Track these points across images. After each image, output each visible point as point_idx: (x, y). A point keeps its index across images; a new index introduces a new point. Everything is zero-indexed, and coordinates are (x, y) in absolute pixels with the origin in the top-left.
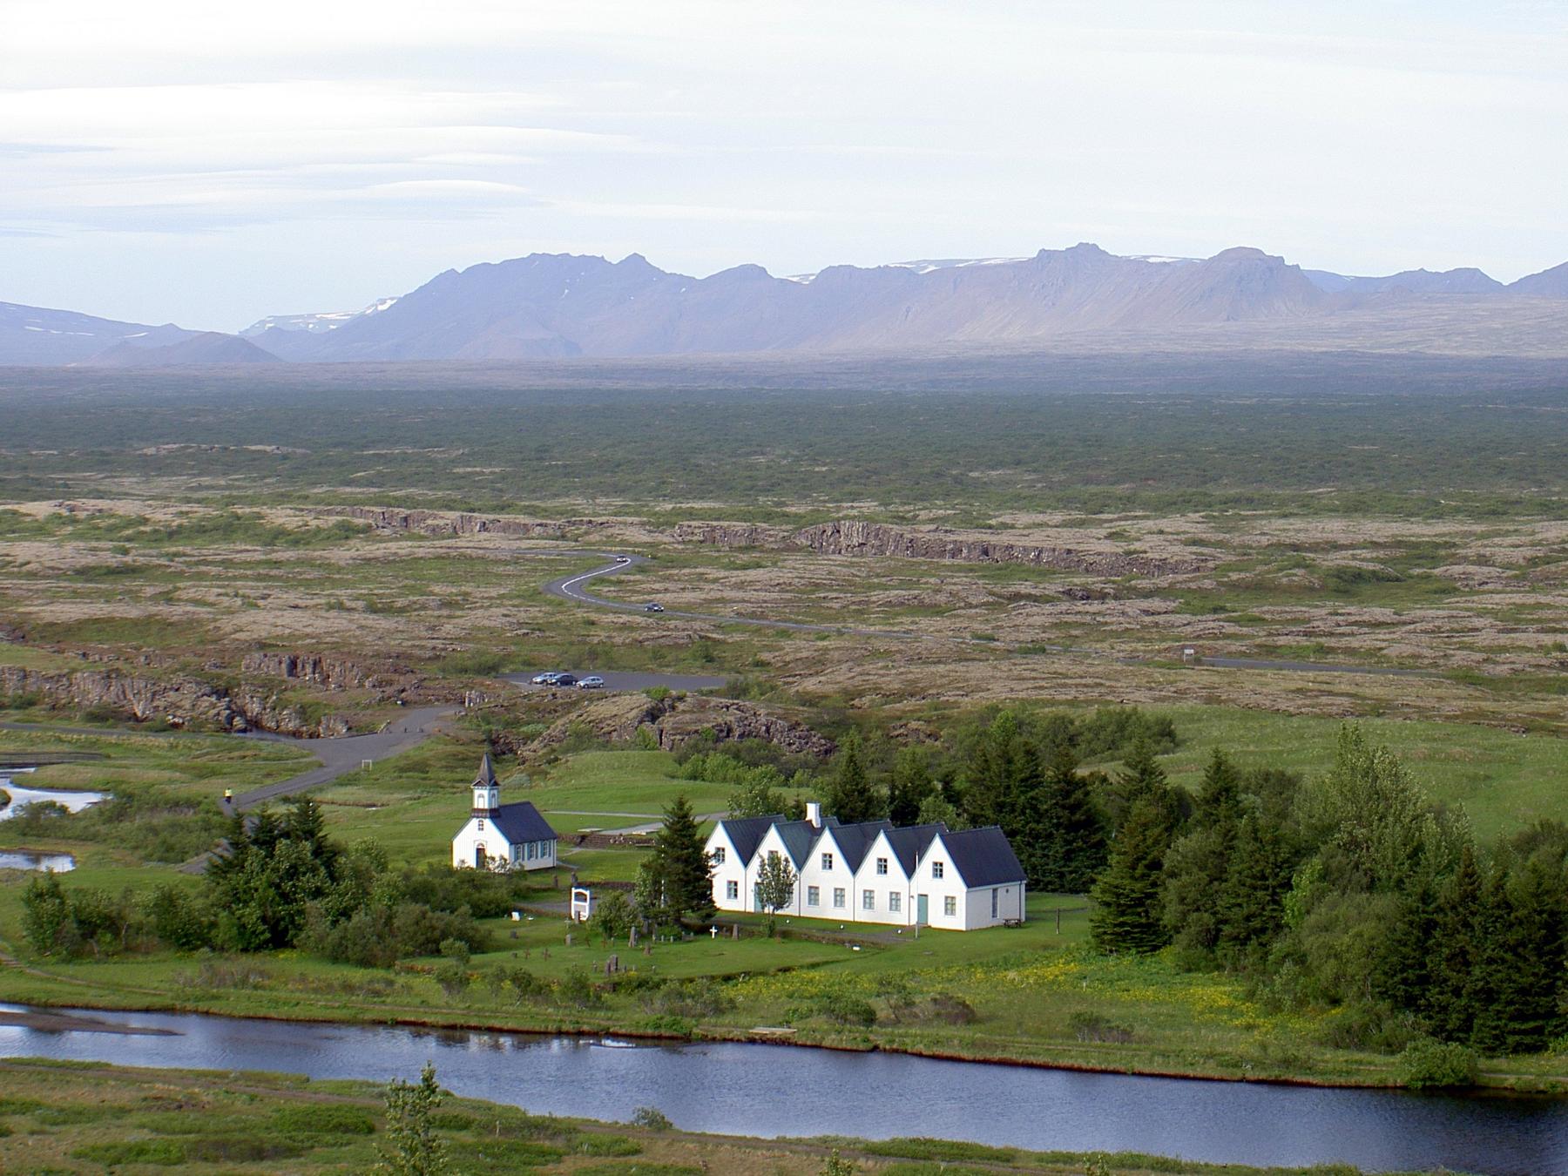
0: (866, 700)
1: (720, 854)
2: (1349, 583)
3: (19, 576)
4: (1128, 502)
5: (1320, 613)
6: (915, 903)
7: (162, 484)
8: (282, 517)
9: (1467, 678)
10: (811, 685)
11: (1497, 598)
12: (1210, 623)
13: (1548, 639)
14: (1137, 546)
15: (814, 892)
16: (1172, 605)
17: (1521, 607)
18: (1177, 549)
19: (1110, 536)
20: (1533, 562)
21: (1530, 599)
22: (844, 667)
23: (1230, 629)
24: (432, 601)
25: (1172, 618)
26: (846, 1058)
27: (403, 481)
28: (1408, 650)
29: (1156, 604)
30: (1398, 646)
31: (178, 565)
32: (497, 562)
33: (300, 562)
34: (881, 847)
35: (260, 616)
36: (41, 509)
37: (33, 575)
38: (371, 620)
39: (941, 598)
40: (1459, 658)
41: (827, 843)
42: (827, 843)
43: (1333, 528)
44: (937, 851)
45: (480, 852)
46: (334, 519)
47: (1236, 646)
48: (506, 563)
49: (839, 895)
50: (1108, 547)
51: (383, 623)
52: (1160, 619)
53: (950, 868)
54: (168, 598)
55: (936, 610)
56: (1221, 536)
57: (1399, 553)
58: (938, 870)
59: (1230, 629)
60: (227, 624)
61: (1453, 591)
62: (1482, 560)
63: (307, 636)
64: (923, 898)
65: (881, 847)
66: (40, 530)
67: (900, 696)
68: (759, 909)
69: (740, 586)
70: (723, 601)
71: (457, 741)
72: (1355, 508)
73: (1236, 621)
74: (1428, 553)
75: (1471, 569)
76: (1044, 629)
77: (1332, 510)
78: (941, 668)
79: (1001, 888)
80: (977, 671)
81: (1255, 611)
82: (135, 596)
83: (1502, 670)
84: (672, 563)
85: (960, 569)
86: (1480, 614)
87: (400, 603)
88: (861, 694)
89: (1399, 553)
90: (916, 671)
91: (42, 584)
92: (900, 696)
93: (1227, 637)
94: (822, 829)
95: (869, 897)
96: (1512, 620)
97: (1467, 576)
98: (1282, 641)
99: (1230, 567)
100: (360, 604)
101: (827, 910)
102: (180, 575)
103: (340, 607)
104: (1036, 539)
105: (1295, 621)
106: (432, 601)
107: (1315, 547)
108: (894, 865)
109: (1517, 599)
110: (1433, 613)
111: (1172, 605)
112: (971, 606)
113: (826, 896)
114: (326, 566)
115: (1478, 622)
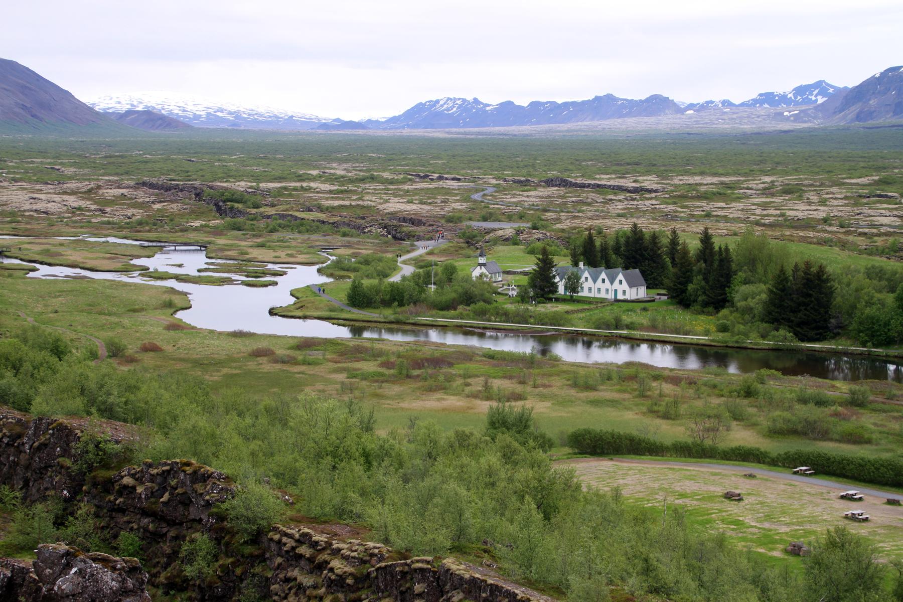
3: (314, 192)
7: (345, 166)
8: (386, 175)
11: (757, 200)
12: (671, 208)
14: (642, 185)
16: (658, 202)
17: (766, 202)
18: (655, 185)
19: (634, 181)
20: (765, 189)
22: (568, 221)
23: (679, 209)
24: (438, 201)
25: (661, 206)
29: (654, 202)
32: (453, 189)
33: (395, 189)
34: (603, 275)
35: (391, 205)
36: (314, 172)
37: (318, 192)
39: (589, 200)
40: (752, 218)
41: (586, 274)
42: (586, 274)
43: (698, 179)
46: (402, 176)
47: (682, 215)
48: (456, 190)
49: (590, 289)
50: (634, 185)
52: (657, 206)
53: (624, 282)
54: (360, 199)
55: (589, 204)
56: (668, 182)
59: (679, 209)
60: (381, 207)
63: (405, 211)
64: (616, 291)
65: (603, 275)
69: (528, 196)
70: (525, 201)
72: (702, 173)
73: (682, 207)
75: (746, 191)
76: (622, 209)
83: (767, 222)
84: (505, 189)
85: (590, 191)
86: (753, 204)
87: (430, 201)
91: (321, 195)
95: (599, 290)
96: (764, 207)
98: (696, 213)
101: (594, 294)
104: (612, 183)
106: (438, 201)
110: (740, 205)
111: (658, 202)
112: (597, 202)
114: (403, 190)
115: (753, 207)
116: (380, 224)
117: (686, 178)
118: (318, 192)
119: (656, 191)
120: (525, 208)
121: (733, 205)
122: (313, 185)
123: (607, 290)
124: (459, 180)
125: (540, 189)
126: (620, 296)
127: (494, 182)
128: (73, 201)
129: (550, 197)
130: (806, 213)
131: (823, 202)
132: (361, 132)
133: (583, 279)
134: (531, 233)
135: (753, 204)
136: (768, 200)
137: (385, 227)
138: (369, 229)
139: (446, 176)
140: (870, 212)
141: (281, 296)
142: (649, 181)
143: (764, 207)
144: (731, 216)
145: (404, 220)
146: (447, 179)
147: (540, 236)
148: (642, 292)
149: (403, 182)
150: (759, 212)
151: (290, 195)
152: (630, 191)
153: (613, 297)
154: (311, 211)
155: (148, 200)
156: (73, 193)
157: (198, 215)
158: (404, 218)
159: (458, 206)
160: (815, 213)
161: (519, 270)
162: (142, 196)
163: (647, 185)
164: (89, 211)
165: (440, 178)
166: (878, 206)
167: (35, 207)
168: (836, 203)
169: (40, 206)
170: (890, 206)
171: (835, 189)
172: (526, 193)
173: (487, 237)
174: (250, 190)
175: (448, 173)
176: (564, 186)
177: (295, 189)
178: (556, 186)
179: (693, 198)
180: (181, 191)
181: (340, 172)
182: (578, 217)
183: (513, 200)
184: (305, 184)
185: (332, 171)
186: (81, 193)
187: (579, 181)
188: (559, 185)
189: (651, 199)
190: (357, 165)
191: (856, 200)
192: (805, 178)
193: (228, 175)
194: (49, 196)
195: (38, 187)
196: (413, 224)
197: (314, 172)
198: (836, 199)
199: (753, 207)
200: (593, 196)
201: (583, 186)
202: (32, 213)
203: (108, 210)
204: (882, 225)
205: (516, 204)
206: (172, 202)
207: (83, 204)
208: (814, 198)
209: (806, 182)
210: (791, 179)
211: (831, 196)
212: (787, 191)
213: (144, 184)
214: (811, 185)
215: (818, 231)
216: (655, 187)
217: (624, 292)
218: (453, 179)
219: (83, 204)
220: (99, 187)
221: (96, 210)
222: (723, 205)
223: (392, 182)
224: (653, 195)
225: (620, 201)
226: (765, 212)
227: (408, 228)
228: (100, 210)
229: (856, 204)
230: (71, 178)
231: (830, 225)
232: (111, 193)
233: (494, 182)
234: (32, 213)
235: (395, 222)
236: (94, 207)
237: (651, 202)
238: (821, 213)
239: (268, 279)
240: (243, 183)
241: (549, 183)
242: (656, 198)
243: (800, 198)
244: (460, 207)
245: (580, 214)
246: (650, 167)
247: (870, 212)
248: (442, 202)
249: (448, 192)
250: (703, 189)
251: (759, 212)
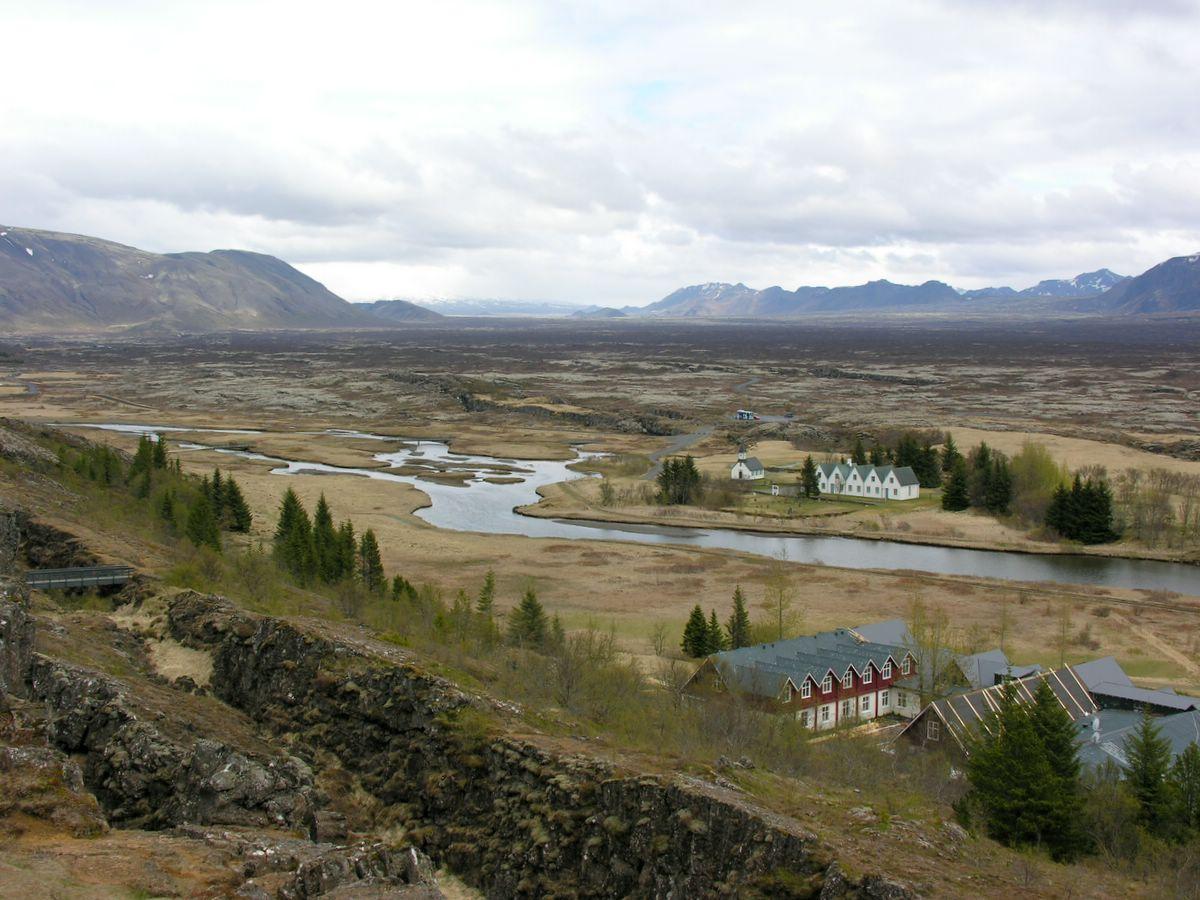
0: (847, 425)
1: (820, 474)
2: (987, 388)
4: (911, 361)
5: (984, 397)
6: (884, 491)
7: (600, 354)
8: (643, 365)
9: (1038, 418)
10: (828, 420)
13: (1061, 406)
14: (918, 376)
15: (850, 487)
19: (910, 372)
20: (1048, 381)
21: (1050, 393)
22: (837, 414)
23: (957, 402)
24: (699, 392)
25: (939, 399)
26: (870, 542)
27: (675, 354)
28: (1017, 410)
29: (930, 394)
30: (1014, 408)
31: (614, 380)
33: (652, 380)
34: (873, 473)
35: (647, 396)
36: (566, 363)
37: (570, 383)
38: (681, 398)
39: (860, 392)
40: (1034, 412)
42: (855, 472)
44: (891, 474)
45: (741, 473)
47: (960, 408)
49: (859, 488)
50: (909, 376)
51: (685, 399)
53: (895, 480)
54: (612, 391)
55: (860, 396)
57: (1004, 378)
58: (892, 480)
59: (957, 402)
60: (635, 399)
61: (1023, 391)
62: (1030, 381)
65: (873, 473)
66: (567, 369)
67: (857, 424)
68: (943, 487)
69: (794, 388)
71: (717, 437)
72: (983, 363)
74: (1013, 378)
77: (975, 365)
78: (870, 415)
79: (912, 487)
80: (881, 416)
81: (962, 397)
82: (604, 390)
83: (1049, 416)
86: (1036, 397)
87: (689, 392)
88: (844, 423)
89: (1004, 378)
90: (862, 416)
92: (857, 424)
93: (957, 405)
94: (853, 467)
95: (869, 489)
96: (1047, 400)
97: (1028, 386)
99: (949, 383)
100: (676, 393)
102: (616, 384)
103: (670, 394)
105: (977, 400)
107: (976, 376)
108: (877, 479)
109: (1047, 393)
113: (855, 488)
114: (661, 381)
116: (635, 417)
117: (965, 368)
118: (570, 383)
119: (933, 382)
120: (791, 401)
121: (1015, 398)
123: (877, 489)
124: (721, 370)
125: (808, 379)
126: (891, 496)
127: (759, 372)
128: (319, 395)
129: (819, 388)
130: (1090, 407)
131: (1108, 397)
132: (618, 319)
133: (851, 476)
135: (1036, 397)
136: (1050, 393)
137: (640, 420)
138: (623, 422)
139: (707, 366)
140: (1157, 407)
141: (524, 494)
142: (926, 372)
143: (1047, 400)
144: (1011, 410)
145: (661, 413)
146: (708, 369)
148: (915, 491)
149: (663, 371)
150: (1041, 406)
151: (540, 387)
152: (904, 383)
153: (884, 496)
154: (563, 403)
155: (392, 392)
156: (319, 386)
157: (443, 407)
158: (660, 411)
159: (721, 397)
160: (1100, 407)
161: (785, 467)
162: (387, 388)
163: (923, 376)
164: (335, 404)
166: (1165, 401)
167: (282, 401)
168: (1121, 397)
169: (287, 400)
170: (1176, 402)
171: (1120, 383)
172: (793, 384)
173: (750, 431)
174: (498, 382)
175: (710, 363)
176: (835, 377)
177: (546, 381)
178: (825, 376)
179: (974, 390)
180: (428, 382)
181: (594, 362)
182: (848, 410)
183: (781, 391)
184: (555, 375)
185: (586, 361)
186: (327, 386)
187: (850, 371)
188: (829, 376)
190: (613, 354)
191: (1141, 395)
192: (1087, 370)
194: (296, 390)
195: (287, 380)
196: (670, 417)
197: (566, 363)
198: (1121, 393)
199: (1036, 401)
200: (865, 387)
201: (854, 376)
202: (278, 408)
203: (353, 403)
204: (1167, 422)
205: (780, 396)
206: (417, 394)
207: (329, 397)
208: (1098, 392)
209: (1090, 375)
210: (1074, 372)
211: (1116, 390)
212: (1074, 382)
213: (390, 376)
214: (1096, 378)
215: (1104, 427)
216: (931, 377)
217: (896, 491)
218: (715, 369)
219: (329, 397)
220: (345, 380)
222: (1004, 398)
223: (649, 372)
224: (930, 387)
225: (893, 393)
226: (1047, 406)
227: (664, 421)
228: (345, 404)
229: (1142, 399)
230: (319, 370)
231: (1115, 420)
232: (356, 386)
233: (759, 372)
234: (278, 408)
235: (651, 415)
236: (339, 401)
237: (926, 394)
238: (1107, 407)
239: (514, 475)
240: (491, 375)
242: (932, 390)
243: (1084, 392)
244: (722, 399)
245: (851, 407)
247: (1157, 407)
248: (702, 394)
249: (710, 382)
250: (983, 380)
251: (1041, 406)
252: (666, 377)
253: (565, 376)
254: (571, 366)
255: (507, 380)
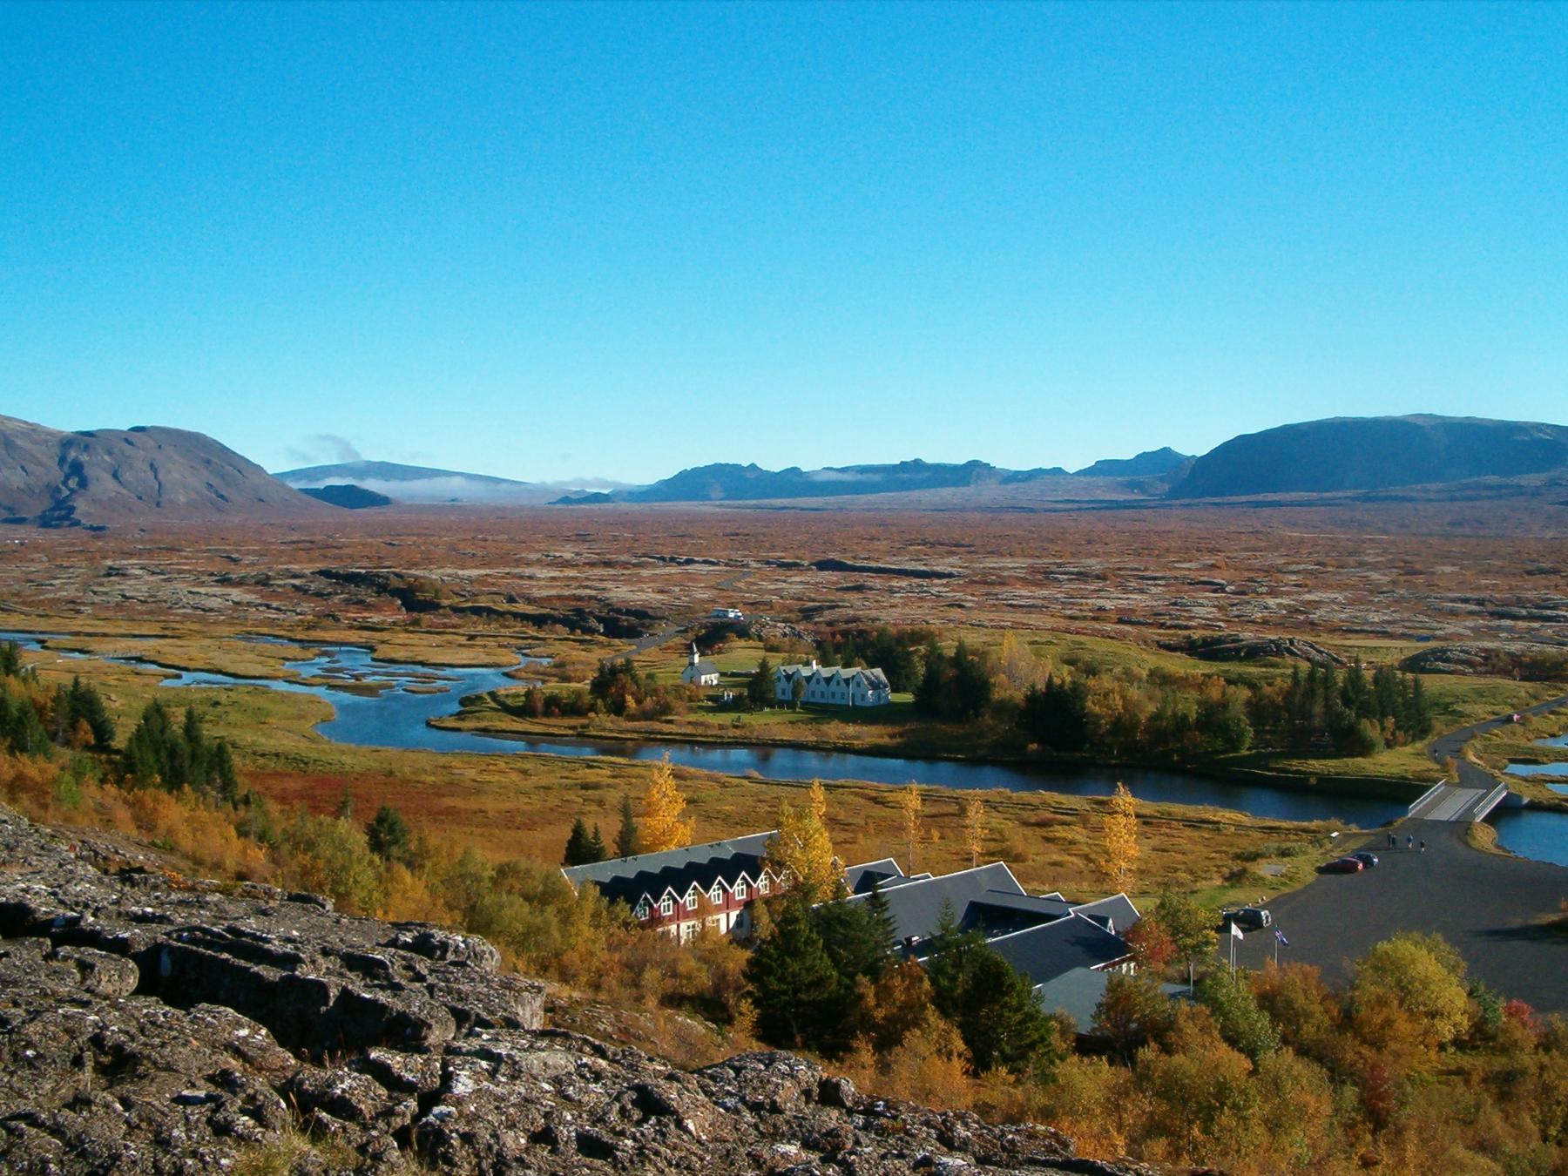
91: (534, 583)
95: (833, 694)
103: (643, 591)
119: (950, 575)
122: (528, 571)
134: (775, 627)
147: (787, 630)
165: (689, 562)
181: (568, 556)
189: (943, 585)
193: (428, 561)
197: (533, 556)
218: (705, 562)
221: (261, 605)
223: (625, 565)
236: (259, 601)
241: (823, 565)
246: (954, 547)
249: (692, 577)
252: (645, 573)
253: (528, 571)
254: (539, 561)
255: (457, 576)
